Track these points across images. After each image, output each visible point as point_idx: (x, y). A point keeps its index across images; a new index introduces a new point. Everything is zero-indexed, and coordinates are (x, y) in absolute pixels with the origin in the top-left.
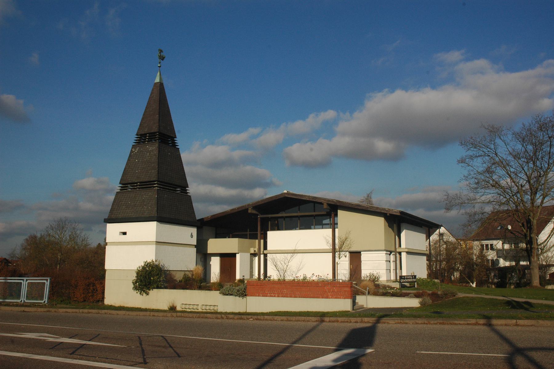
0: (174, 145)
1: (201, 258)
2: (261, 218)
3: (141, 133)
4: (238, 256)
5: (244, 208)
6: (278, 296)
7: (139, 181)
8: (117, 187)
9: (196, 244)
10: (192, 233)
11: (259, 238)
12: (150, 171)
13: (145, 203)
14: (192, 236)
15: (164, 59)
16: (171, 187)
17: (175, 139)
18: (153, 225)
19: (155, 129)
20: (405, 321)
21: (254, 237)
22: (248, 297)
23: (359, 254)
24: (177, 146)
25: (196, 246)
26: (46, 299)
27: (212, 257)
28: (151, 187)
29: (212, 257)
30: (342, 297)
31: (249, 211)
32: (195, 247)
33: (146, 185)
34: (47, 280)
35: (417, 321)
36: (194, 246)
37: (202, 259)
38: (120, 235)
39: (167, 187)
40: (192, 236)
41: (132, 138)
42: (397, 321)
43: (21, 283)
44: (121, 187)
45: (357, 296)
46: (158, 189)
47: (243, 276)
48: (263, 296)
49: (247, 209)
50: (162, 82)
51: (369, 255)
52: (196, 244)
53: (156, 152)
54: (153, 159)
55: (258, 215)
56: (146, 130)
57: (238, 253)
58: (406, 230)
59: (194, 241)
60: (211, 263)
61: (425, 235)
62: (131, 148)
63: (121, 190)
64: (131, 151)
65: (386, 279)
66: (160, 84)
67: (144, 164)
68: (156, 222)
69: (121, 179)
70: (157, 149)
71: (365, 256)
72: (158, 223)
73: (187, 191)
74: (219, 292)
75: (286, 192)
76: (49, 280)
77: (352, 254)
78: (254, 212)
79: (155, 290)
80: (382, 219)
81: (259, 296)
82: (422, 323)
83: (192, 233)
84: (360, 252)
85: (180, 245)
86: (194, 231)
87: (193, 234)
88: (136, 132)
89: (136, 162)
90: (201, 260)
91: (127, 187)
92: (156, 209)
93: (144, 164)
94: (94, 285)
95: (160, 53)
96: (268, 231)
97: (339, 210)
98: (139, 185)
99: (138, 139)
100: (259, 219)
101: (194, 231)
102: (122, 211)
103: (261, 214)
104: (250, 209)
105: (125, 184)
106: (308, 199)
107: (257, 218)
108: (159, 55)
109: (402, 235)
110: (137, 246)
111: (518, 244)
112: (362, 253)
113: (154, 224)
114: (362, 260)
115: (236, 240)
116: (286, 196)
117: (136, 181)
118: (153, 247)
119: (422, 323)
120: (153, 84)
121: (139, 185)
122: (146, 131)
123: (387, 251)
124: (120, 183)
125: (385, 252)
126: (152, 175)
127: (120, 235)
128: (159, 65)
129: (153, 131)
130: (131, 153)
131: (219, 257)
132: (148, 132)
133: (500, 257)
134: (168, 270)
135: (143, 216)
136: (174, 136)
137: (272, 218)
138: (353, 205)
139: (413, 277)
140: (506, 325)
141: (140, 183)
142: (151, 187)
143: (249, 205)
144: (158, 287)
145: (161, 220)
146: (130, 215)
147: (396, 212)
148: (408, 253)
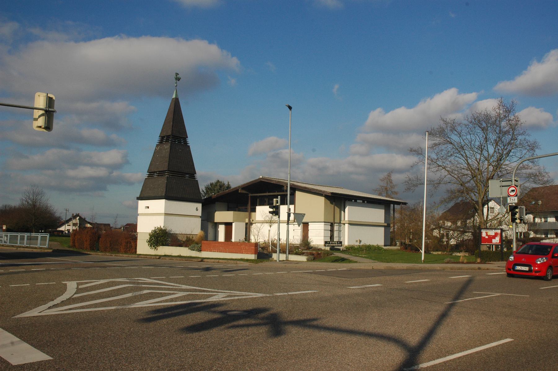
0: (186, 143)
1: (212, 226)
2: (251, 196)
3: (162, 136)
4: (234, 224)
5: (236, 189)
6: (218, 252)
7: (157, 170)
8: (145, 175)
9: (201, 215)
10: (197, 208)
11: (249, 211)
12: (164, 164)
13: (160, 186)
14: (197, 209)
15: (180, 80)
16: (179, 174)
17: (187, 139)
18: (162, 202)
19: (169, 133)
20: (173, 259)
21: (245, 210)
22: (202, 252)
23: (307, 224)
24: (188, 144)
25: (201, 217)
26: (47, 246)
27: (219, 225)
28: (163, 175)
29: (219, 225)
30: (217, 251)
31: (239, 192)
32: (200, 218)
33: (161, 173)
34: (48, 235)
35: (177, 259)
36: (199, 217)
37: (213, 227)
38: (145, 208)
39: (177, 175)
40: (197, 209)
41: (157, 139)
42: (169, 258)
43: (38, 236)
44: (148, 175)
45: (273, 254)
46: (167, 177)
47: (240, 240)
48: (210, 251)
49: (238, 190)
50: (177, 97)
51: (312, 225)
52: (201, 215)
53: (169, 150)
54: (167, 155)
55: (248, 194)
56: (164, 134)
57: (234, 222)
58: (349, 206)
59: (199, 213)
60: (219, 229)
61: (384, 210)
62: (155, 147)
63: (148, 177)
64: (156, 149)
65: (347, 244)
66: (176, 100)
67: (161, 158)
68: (164, 200)
69: (148, 169)
70: (170, 147)
71: (311, 226)
72: (166, 200)
73: (195, 177)
74: (188, 248)
75: (262, 177)
76: (49, 235)
77: (305, 224)
78: (244, 192)
79: (161, 247)
80: (322, 199)
81: (208, 251)
82: (179, 260)
83: (197, 208)
84: (308, 223)
85: (184, 216)
86: (199, 206)
87: (198, 208)
88: (159, 135)
89: (157, 157)
90: (212, 227)
91: (153, 174)
92: (165, 190)
93: (161, 158)
94: (130, 243)
95: (177, 76)
96: (257, 206)
97: (297, 191)
98: (158, 174)
99: (160, 140)
100: (249, 197)
101: (199, 206)
102: (147, 192)
103: (251, 194)
104: (240, 189)
105: (151, 173)
106: (275, 183)
107: (248, 197)
108: (176, 77)
109: (346, 210)
110: (154, 216)
111: (547, 218)
112: (309, 224)
113: (163, 201)
114: (309, 229)
115: (231, 213)
116: (262, 180)
117: (156, 171)
118: (162, 217)
119: (179, 260)
120: (171, 99)
121: (158, 174)
122: (164, 134)
123: (325, 222)
124: (148, 172)
125: (323, 223)
126: (165, 167)
127: (145, 208)
128: (176, 85)
129: (168, 134)
130: (155, 150)
131: (224, 225)
132: (165, 135)
133: (530, 230)
134: (175, 234)
135: (158, 195)
136: (185, 137)
137: (260, 196)
138: (302, 187)
139: (339, 242)
140: (214, 262)
141: (159, 172)
142: (163, 175)
143: (239, 187)
144: (163, 245)
145: (168, 197)
146: (151, 194)
147: (328, 193)
148: (351, 224)
